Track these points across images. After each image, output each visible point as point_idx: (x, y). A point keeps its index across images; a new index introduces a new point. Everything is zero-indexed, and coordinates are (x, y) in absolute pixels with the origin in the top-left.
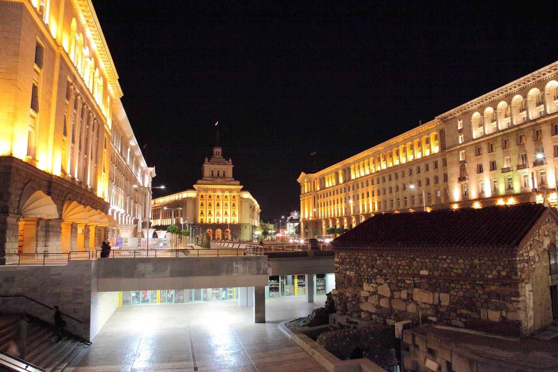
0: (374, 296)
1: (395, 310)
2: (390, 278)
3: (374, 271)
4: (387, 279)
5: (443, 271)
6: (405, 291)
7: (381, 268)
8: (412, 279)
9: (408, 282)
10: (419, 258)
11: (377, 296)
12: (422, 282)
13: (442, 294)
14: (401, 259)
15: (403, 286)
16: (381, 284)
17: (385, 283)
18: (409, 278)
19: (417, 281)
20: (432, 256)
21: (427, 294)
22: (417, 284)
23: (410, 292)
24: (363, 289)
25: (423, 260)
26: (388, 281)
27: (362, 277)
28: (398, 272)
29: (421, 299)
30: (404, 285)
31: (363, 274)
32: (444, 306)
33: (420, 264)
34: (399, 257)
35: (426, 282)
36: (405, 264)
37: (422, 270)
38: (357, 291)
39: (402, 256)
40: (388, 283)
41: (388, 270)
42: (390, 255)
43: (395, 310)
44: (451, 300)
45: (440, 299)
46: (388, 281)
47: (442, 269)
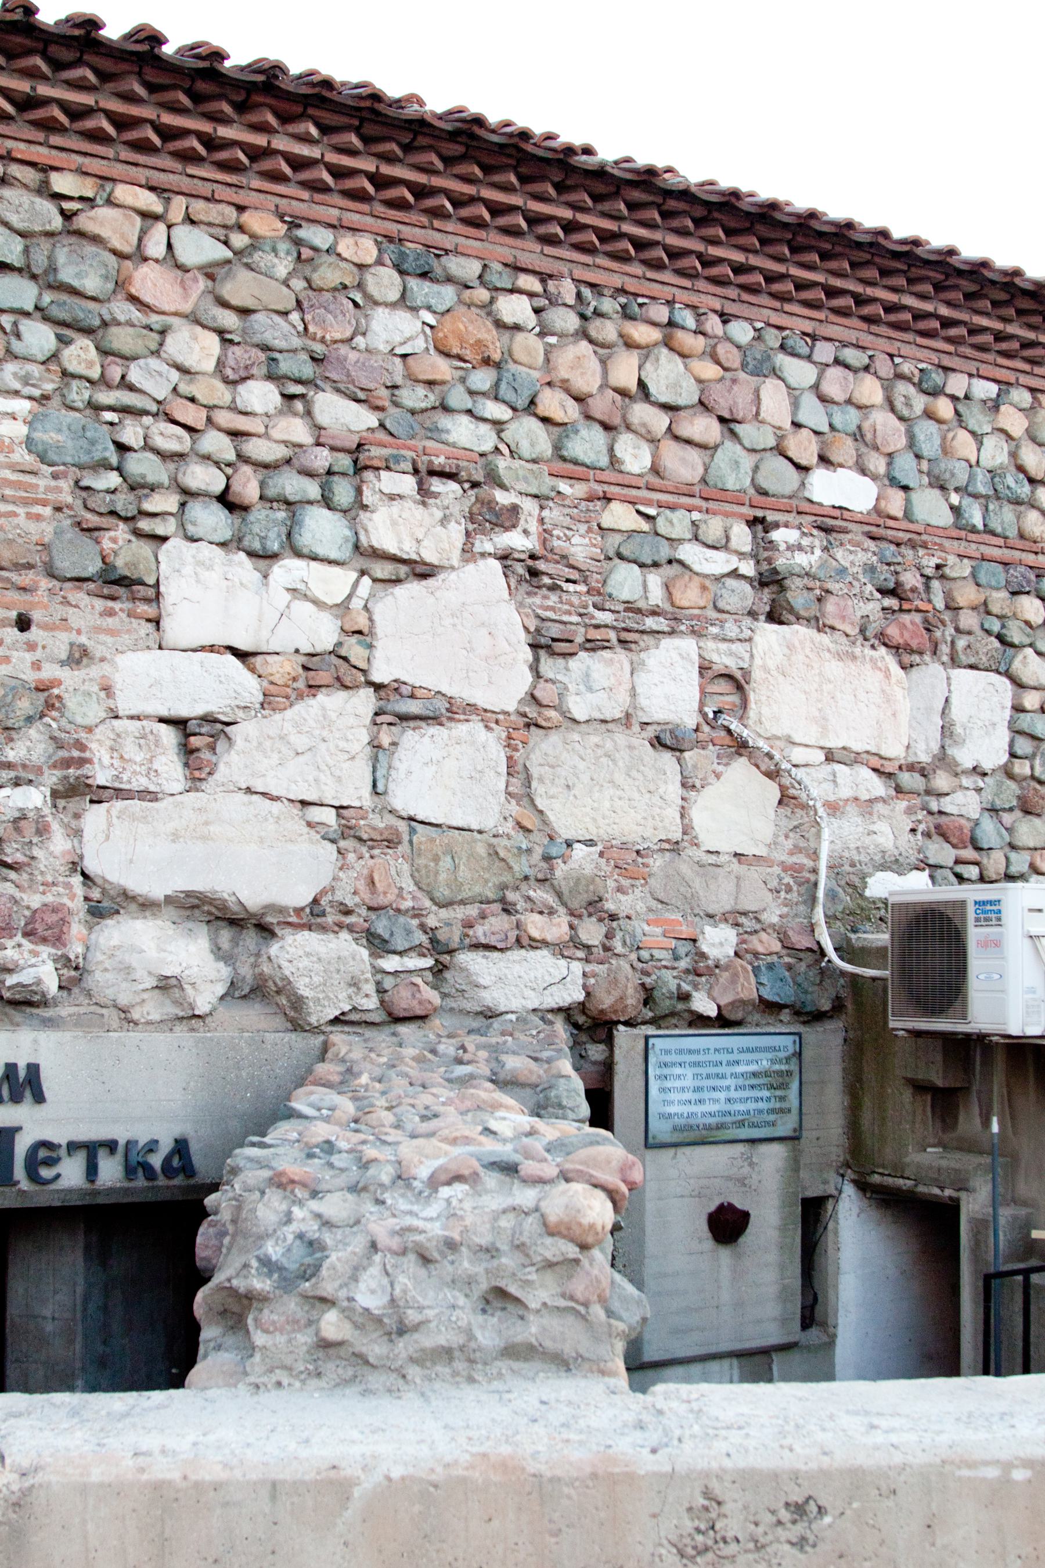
0: (331, 701)
1: (569, 844)
2: (529, 506)
3: (322, 419)
4: (508, 518)
5: (975, 496)
6: (688, 645)
7: (415, 397)
8: (742, 536)
9: (718, 563)
10: (809, 358)
11: (365, 701)
12: (843, 571)
13: (962, 676)
14: (643, 333)
15: (657, 596)
16: (423, 571)
17: (468, 553)
18: (713, 529)
19: (802, 560)
20: (907, 368)
21: (872, 679)
22: (798, 597)
23: (724, 657)
24: (156, 622)
25: (835, 383)
26: (515, 540)
27: (142, 465)
28: (614, 460)
29: (823, 722)
30: (667, 587)
31: (170, 437)
32: (978, 771)
33: (813, 414)
34: (627, 315)
35: (870, 569)
36: (688, 394)
37: (824, 460)
38: (60, 644)
39: (661, 313)
40: (504, 557)
41: (498, 425)
42: (536, 286)
43: (569, 844)
44: (1025, 721)
45: (957, 713)
46: (515, 540)
47: (971, 477)
